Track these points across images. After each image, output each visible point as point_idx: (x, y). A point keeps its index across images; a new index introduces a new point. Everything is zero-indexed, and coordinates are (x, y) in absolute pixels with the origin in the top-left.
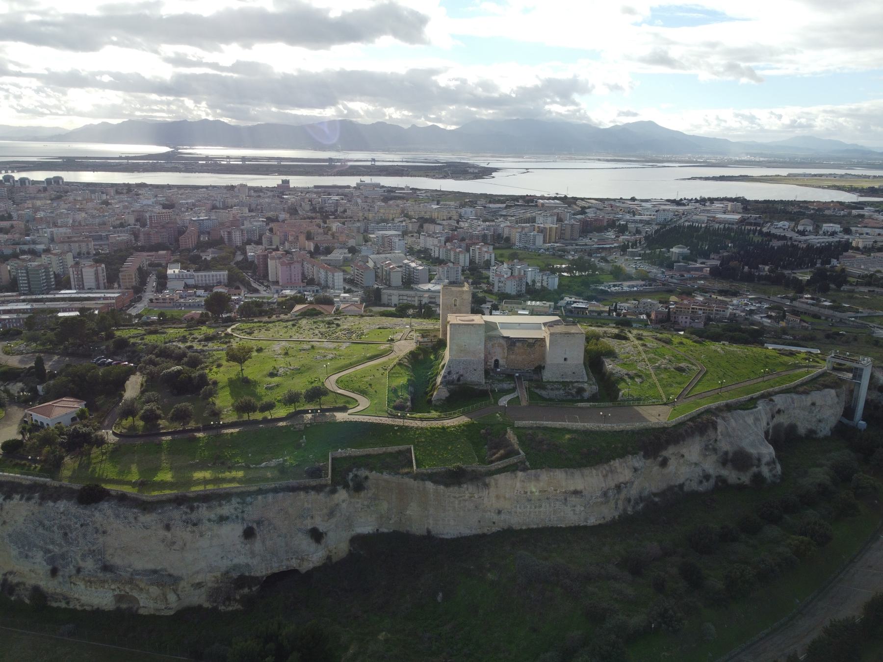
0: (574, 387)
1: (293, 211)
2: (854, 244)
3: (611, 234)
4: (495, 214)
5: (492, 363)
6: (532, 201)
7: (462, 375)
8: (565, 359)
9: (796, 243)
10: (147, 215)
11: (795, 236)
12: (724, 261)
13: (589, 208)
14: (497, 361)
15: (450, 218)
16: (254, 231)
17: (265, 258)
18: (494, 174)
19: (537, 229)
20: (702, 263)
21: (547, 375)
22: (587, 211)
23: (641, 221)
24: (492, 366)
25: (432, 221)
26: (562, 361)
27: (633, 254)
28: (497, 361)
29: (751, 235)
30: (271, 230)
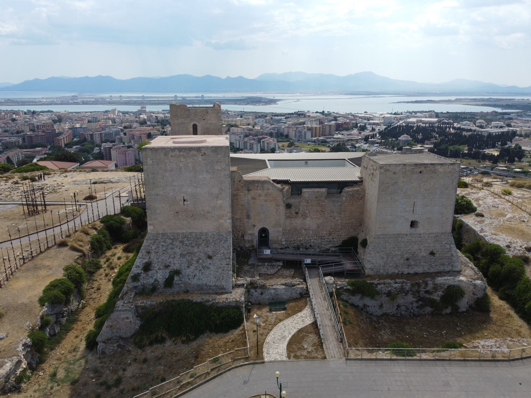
0: (436, 287)
1: (143, 123)
2: (518, 133)
3: (355, 131)
4: (279, 121)
5: (252, 235)
6: (302, 114)
7: (178, 272)
8: (413, 224)
9: (480, 133)
10: (35, 125)
11: (477, 129)
12: (436, 145)
13: (339, 117)
14: (264, 232)
15: (248, 125)
16: (111, 134)
17: (111, 148)
18: (277, 103)
19: (306, 128)
20: (421, 147)
21: (371, 260)
22: (338, 118)
23: (374, 124)
24: (256, 242)
25: (236, 126)
26: (406, 228)
27: (373, 143)
28: (264, 232)
29: (448, 129)
30: (125, 134)
